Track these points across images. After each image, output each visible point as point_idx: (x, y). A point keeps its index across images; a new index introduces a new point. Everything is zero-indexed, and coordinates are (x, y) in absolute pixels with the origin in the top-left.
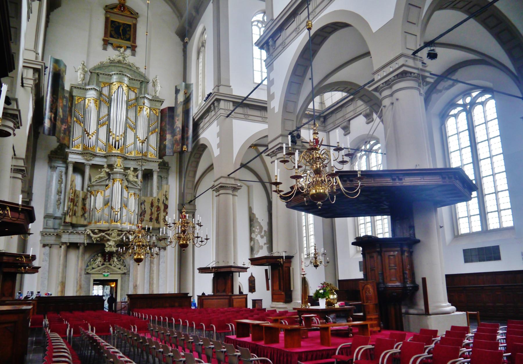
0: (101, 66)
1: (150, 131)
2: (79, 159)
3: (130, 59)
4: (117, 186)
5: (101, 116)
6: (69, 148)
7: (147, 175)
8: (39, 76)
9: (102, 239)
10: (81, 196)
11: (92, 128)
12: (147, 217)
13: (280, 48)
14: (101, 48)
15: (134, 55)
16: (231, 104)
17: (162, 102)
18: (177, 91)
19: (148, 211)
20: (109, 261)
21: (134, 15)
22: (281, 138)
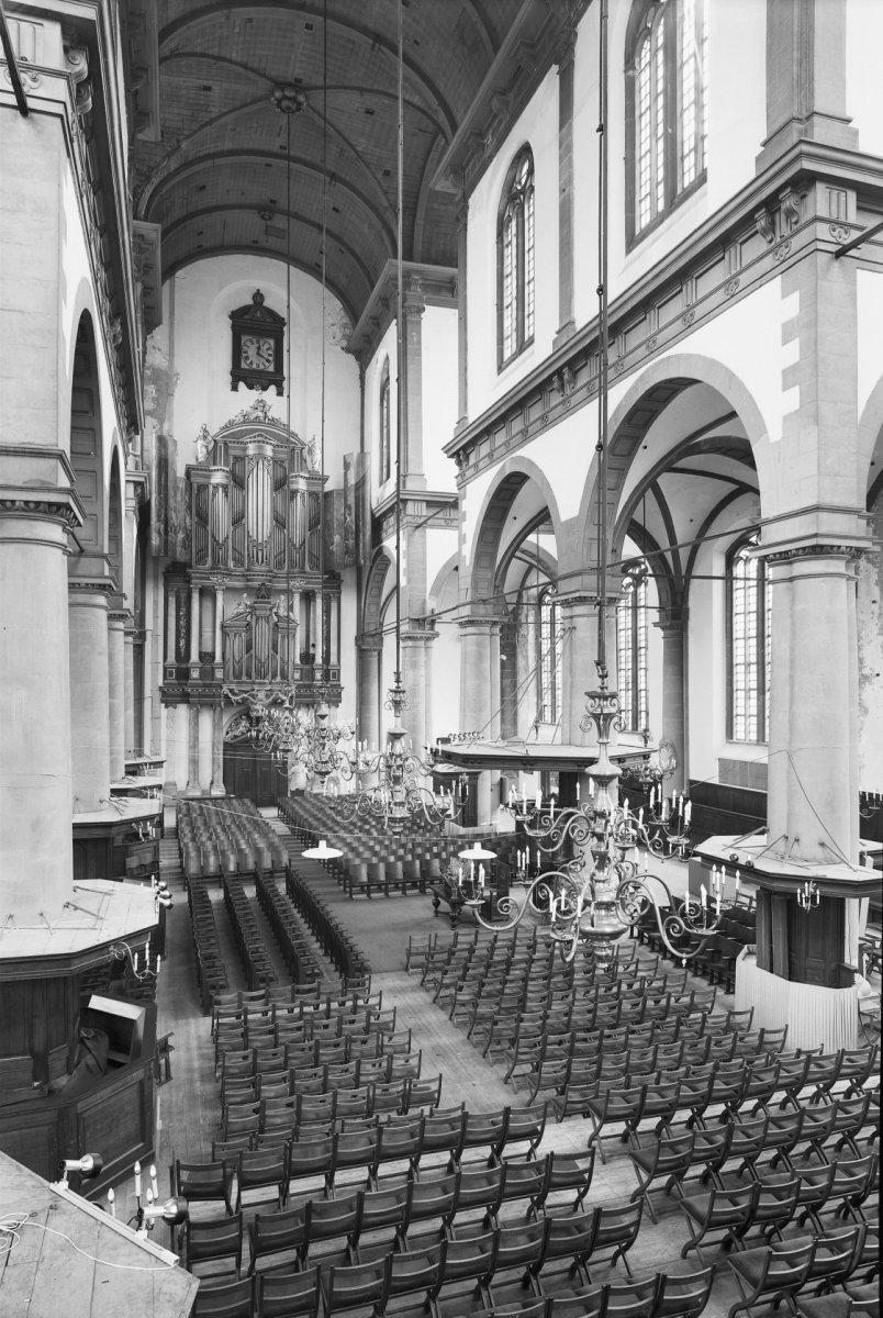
6: (191, 567)
8: (143, 489)
9: (244, 700)
15: (280, 393)
16: (424, 504)
17: (324, 479)
18: (347, 466)
20: (257, 726)
22: (469, 606)
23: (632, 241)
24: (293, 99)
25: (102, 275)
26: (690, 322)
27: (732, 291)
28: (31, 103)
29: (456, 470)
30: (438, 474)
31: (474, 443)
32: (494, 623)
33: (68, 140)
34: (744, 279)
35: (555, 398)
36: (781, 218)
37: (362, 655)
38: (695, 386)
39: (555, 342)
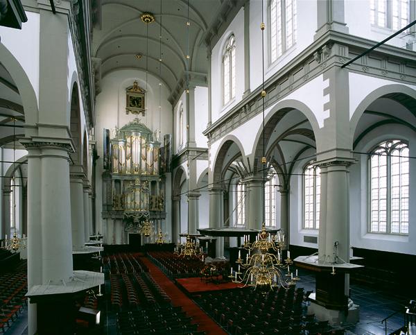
0: (126, 127)
1: (154, 160)
2: (118, 178)
3: (143, 120)
4: (138, 193)
5: (128, 154)
7: (154, 183)
10: (120, 197)
11: (123, 162)
12: (154, 206)
13: (213, 140)
14: (125, 113)
19: (154, 203)
21: (143, 92)
23: (270, 64)
24: (150, 18)
25: (81, 71)
26: (291, 89)
27: (306, 79)
28: (56, 10)
29: (208, 140)
30: (201, 142)
31: (213, 130)
32: (222, 190)
33: (70, 23)
34: (310, 75)
35: (243, 115)
36: (323, 55)
37: (173, 202)
38: (291, 112)
39: (243, 96)
